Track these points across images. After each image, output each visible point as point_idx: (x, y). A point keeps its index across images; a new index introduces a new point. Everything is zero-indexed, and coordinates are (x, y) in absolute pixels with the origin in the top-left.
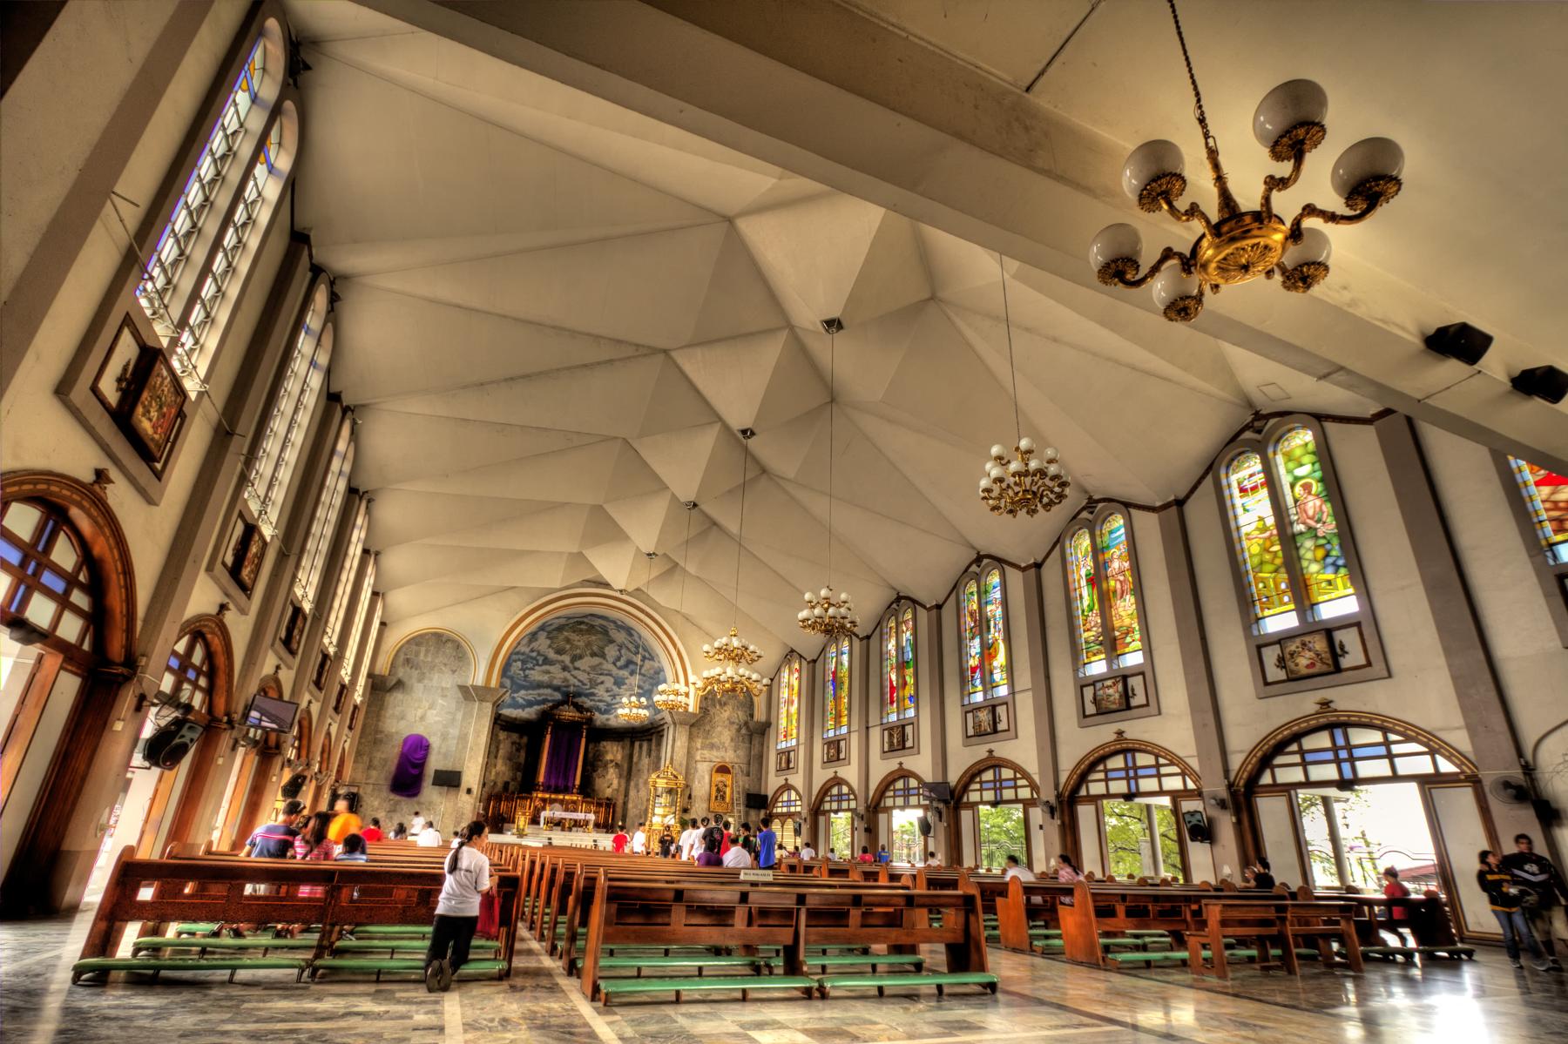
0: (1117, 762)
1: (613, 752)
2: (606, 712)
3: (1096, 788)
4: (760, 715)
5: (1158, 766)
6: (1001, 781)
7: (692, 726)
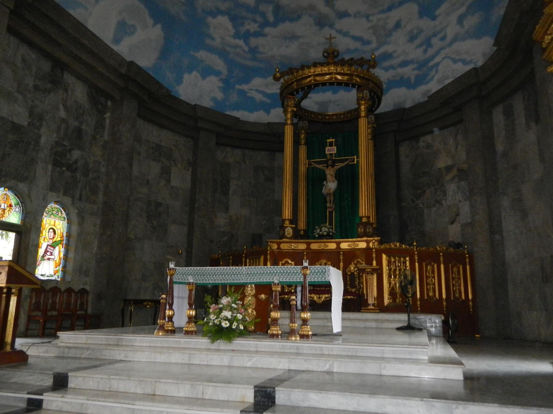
1: (446, 149)
2: (421, 80)
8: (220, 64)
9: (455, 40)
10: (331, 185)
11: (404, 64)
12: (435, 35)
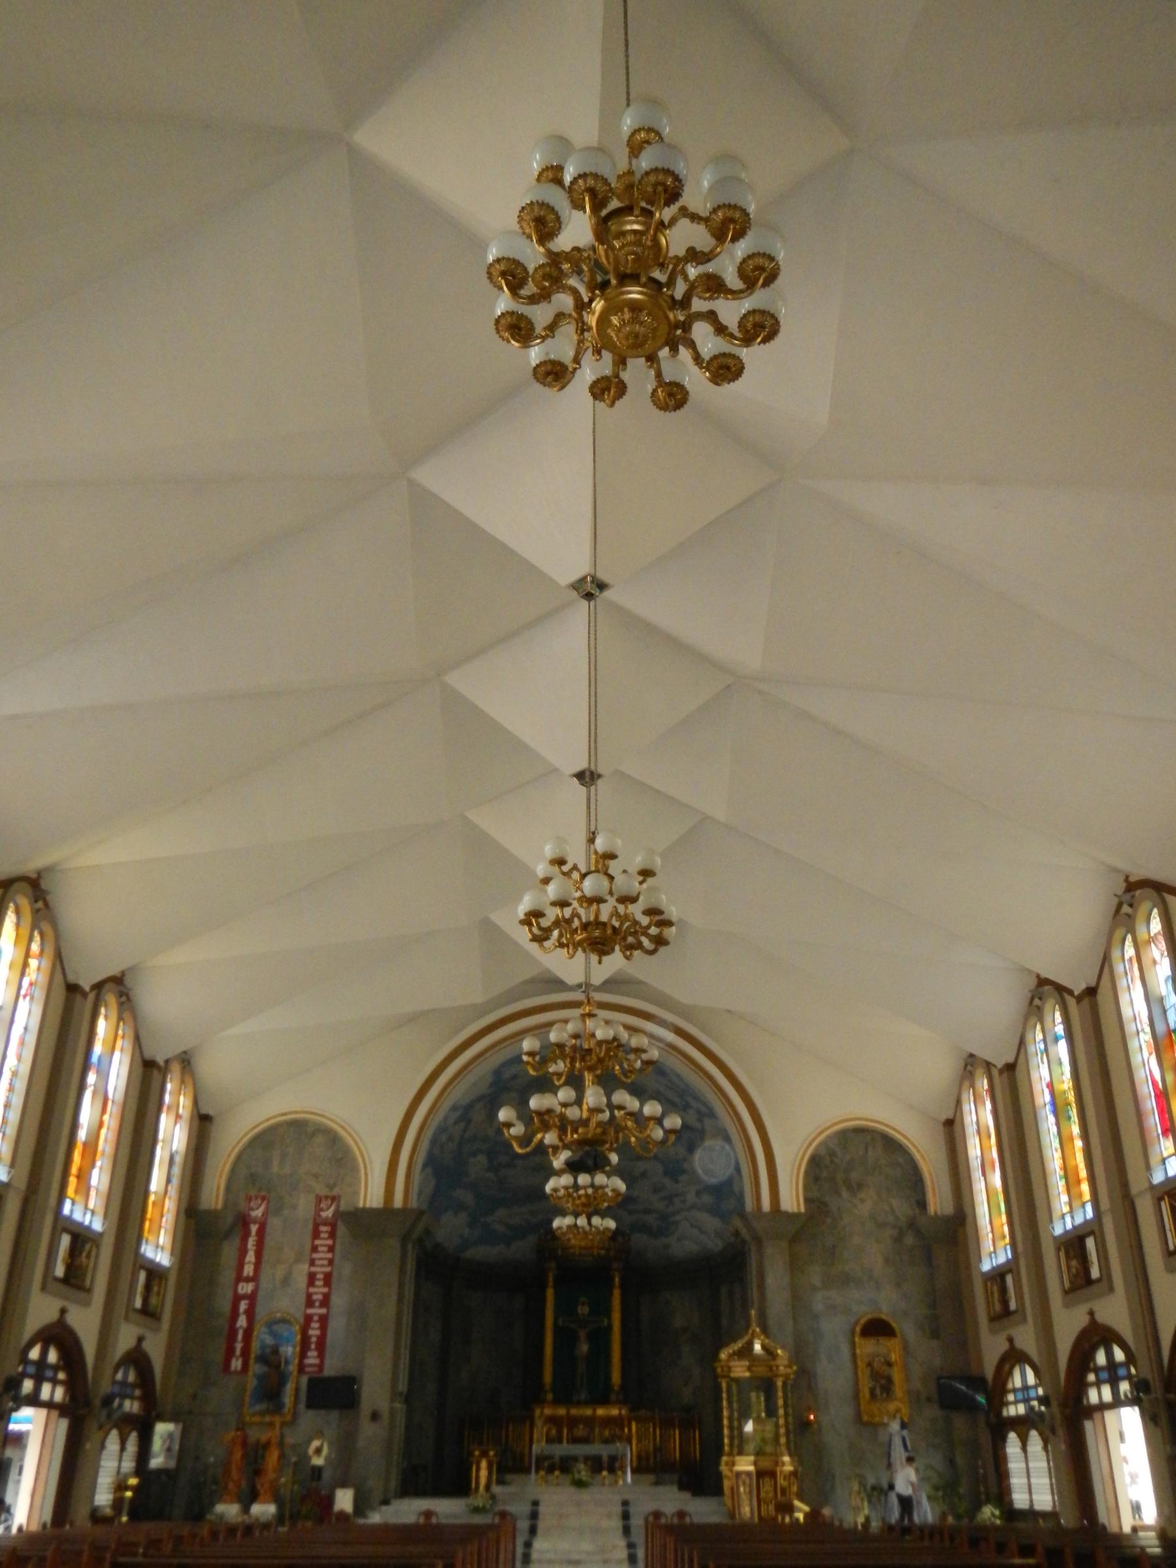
4: (939, 1202)
7: (794, 1240)
8: (468, 1198)
9: (693, 1207)
10: (584, 1348)
11: (648, 1211)
12: (677, 1195)
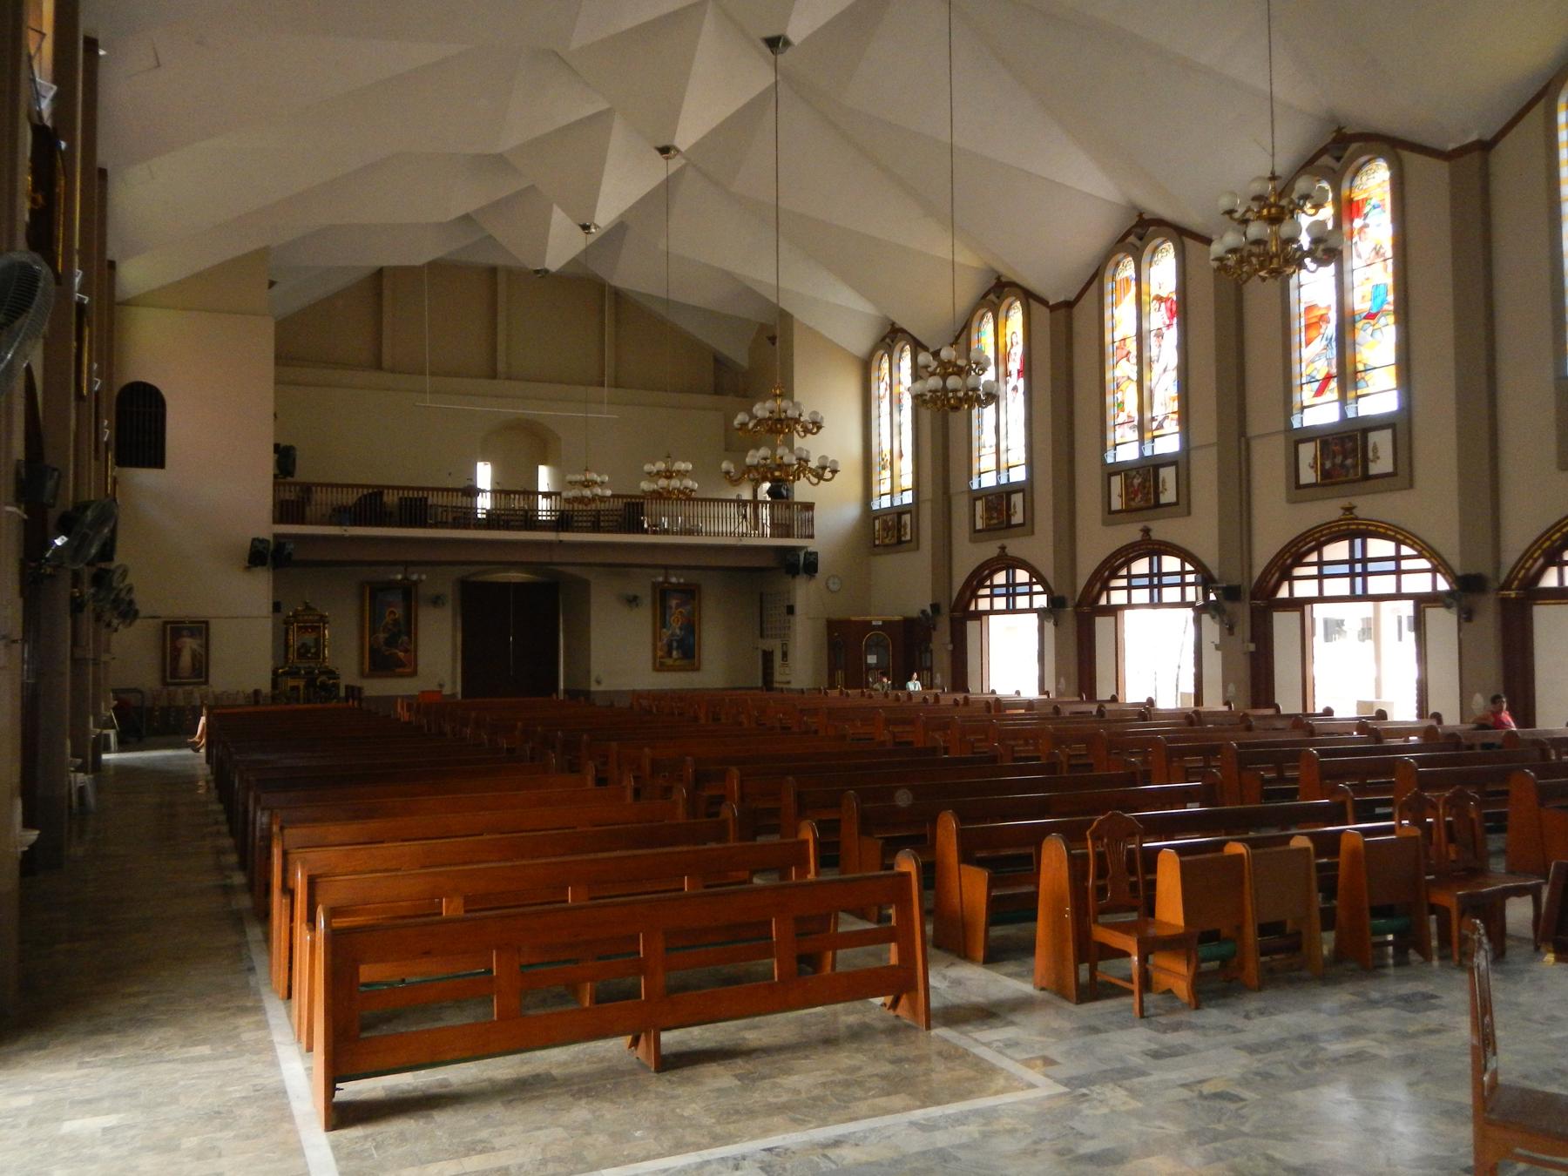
0: (1338, 551)
3: (1304, 589)
5: (1398, 558)
6: (1160, 574)
